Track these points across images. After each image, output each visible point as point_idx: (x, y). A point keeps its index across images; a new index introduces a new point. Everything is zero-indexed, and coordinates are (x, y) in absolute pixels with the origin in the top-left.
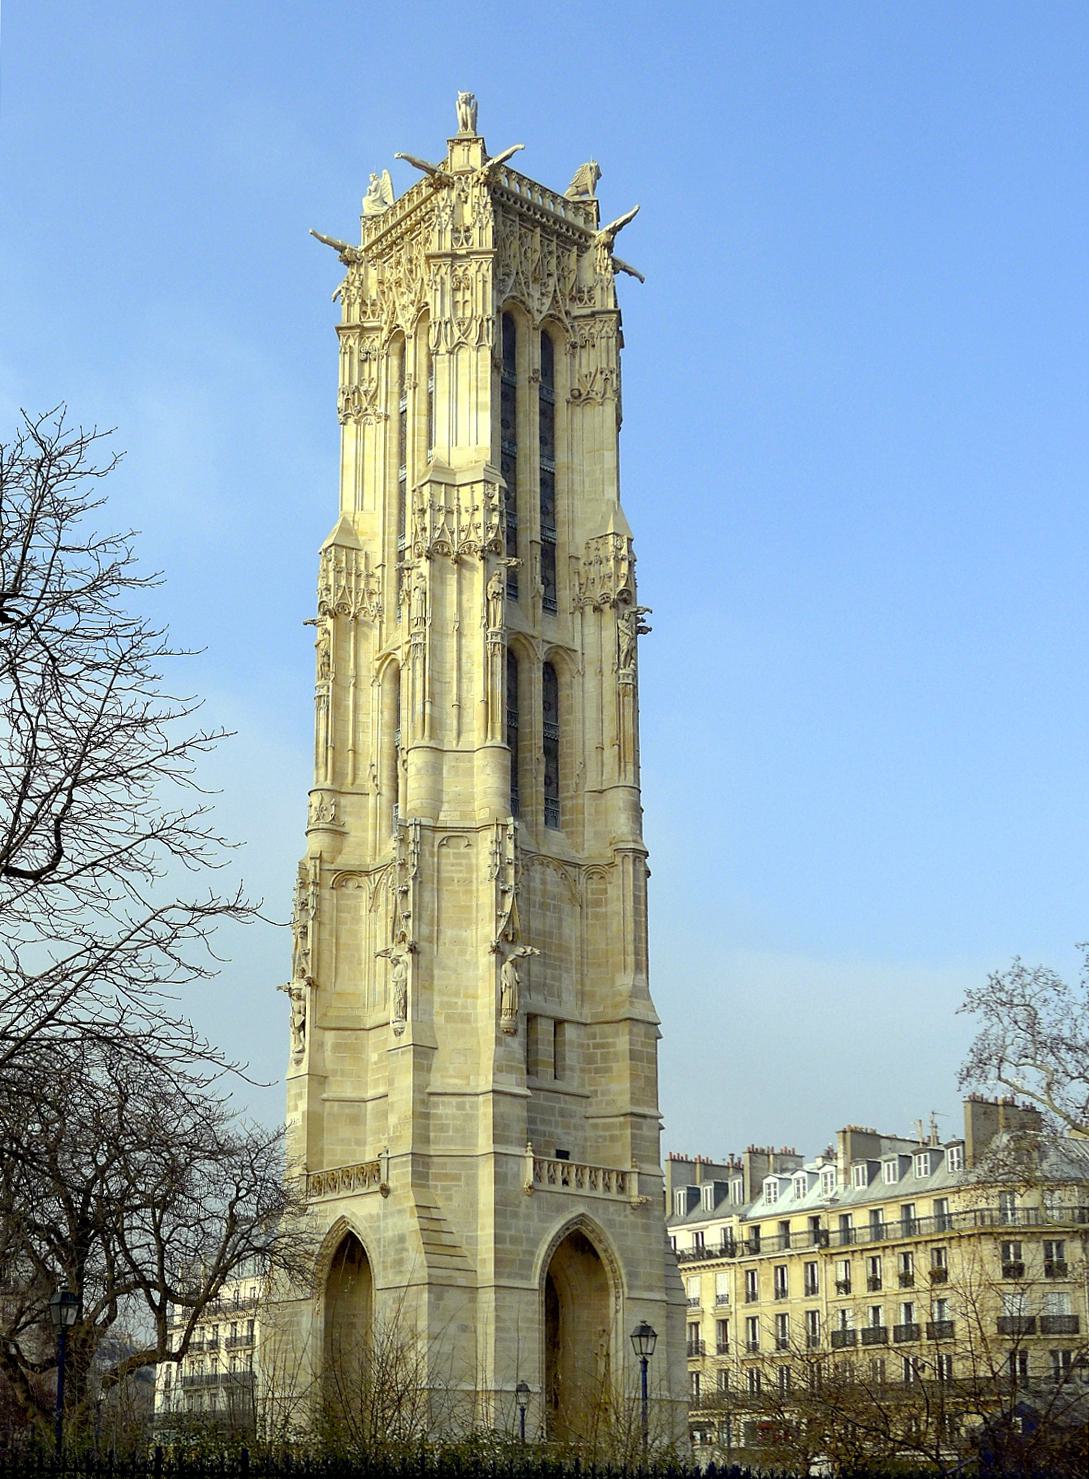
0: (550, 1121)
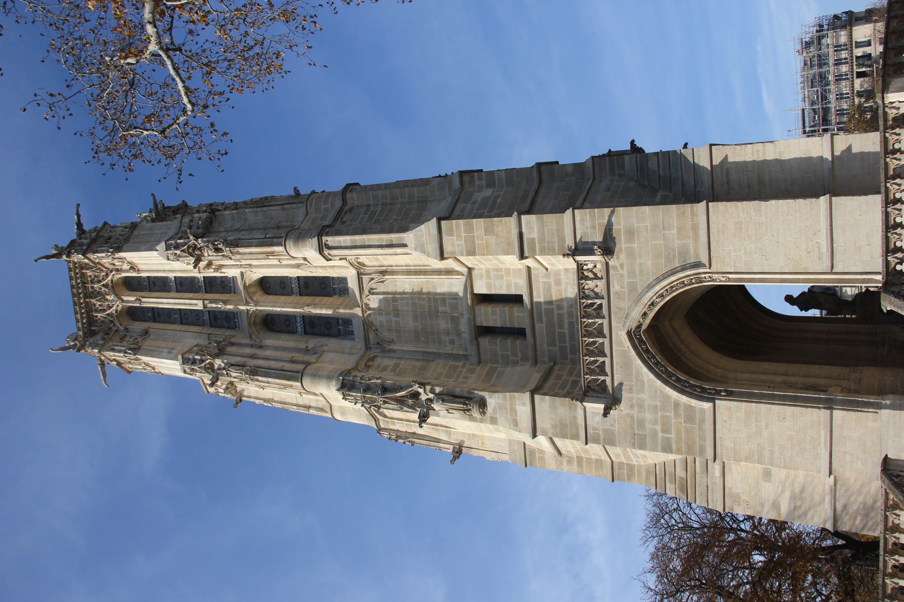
0: (558, 314)
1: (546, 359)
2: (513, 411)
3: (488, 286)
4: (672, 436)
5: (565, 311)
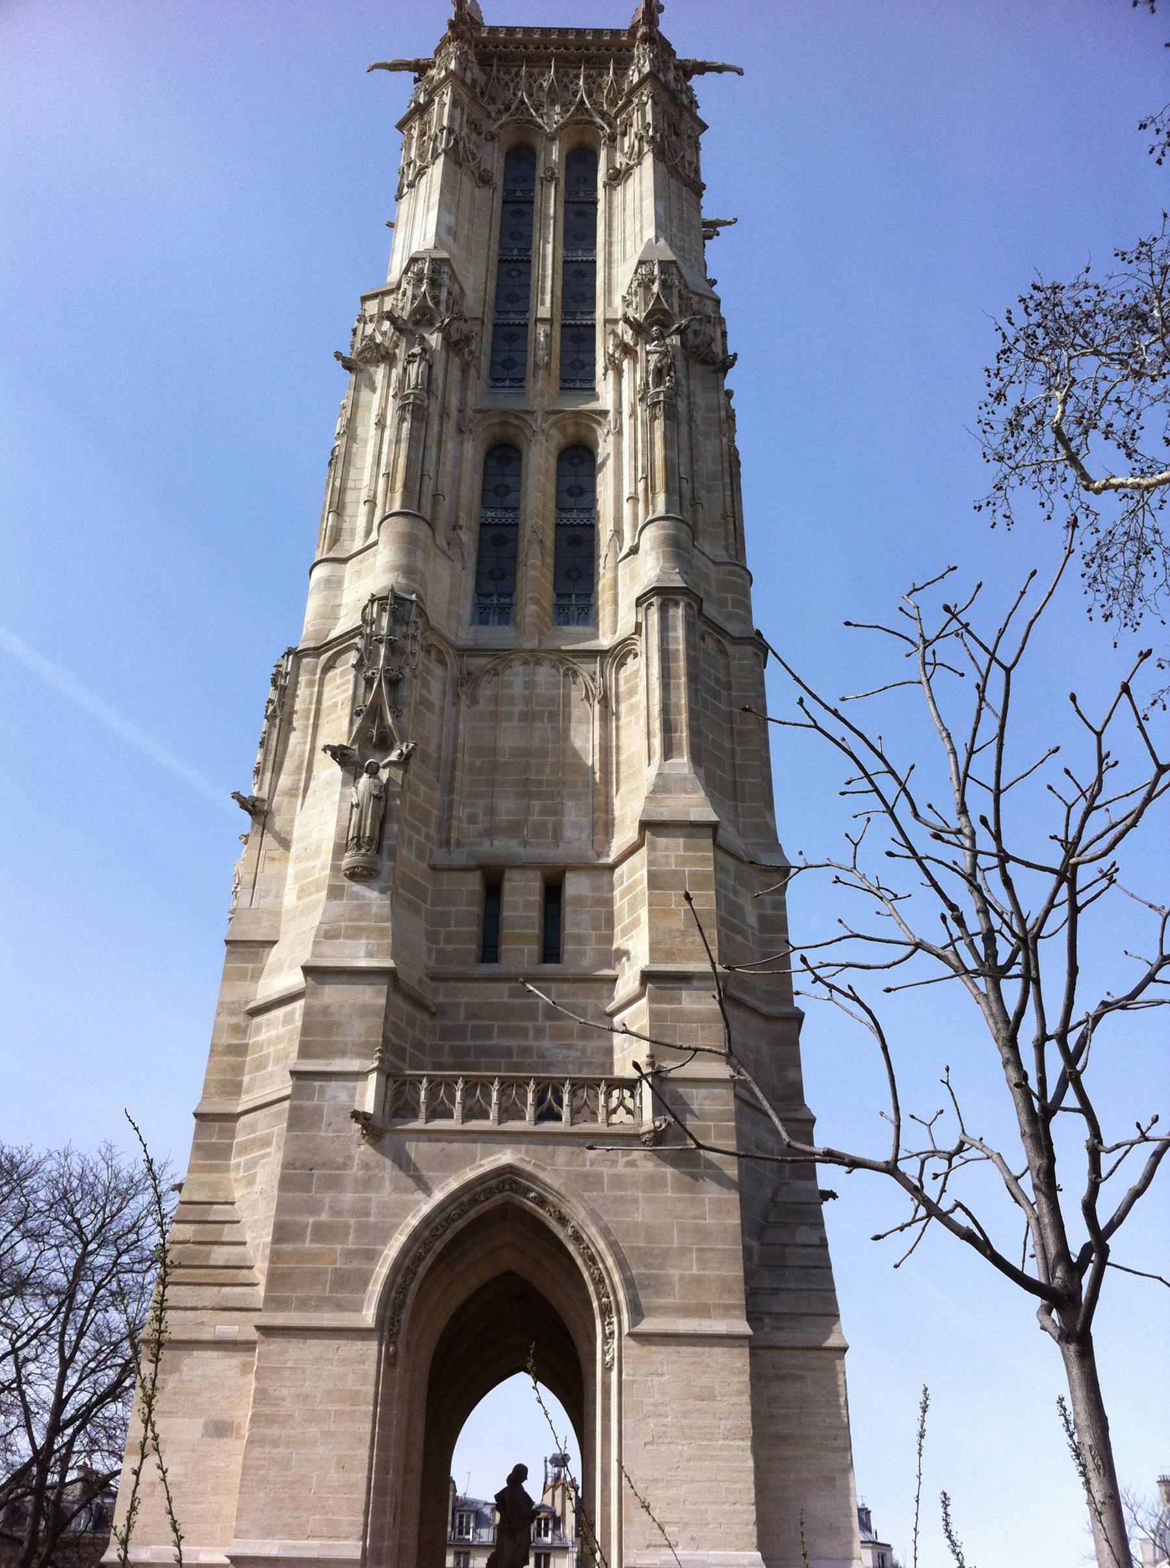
1: (441, 999)
2: (356, 933)
3: (579, 900)
4: (308, 1245)
5: (531, 1042)
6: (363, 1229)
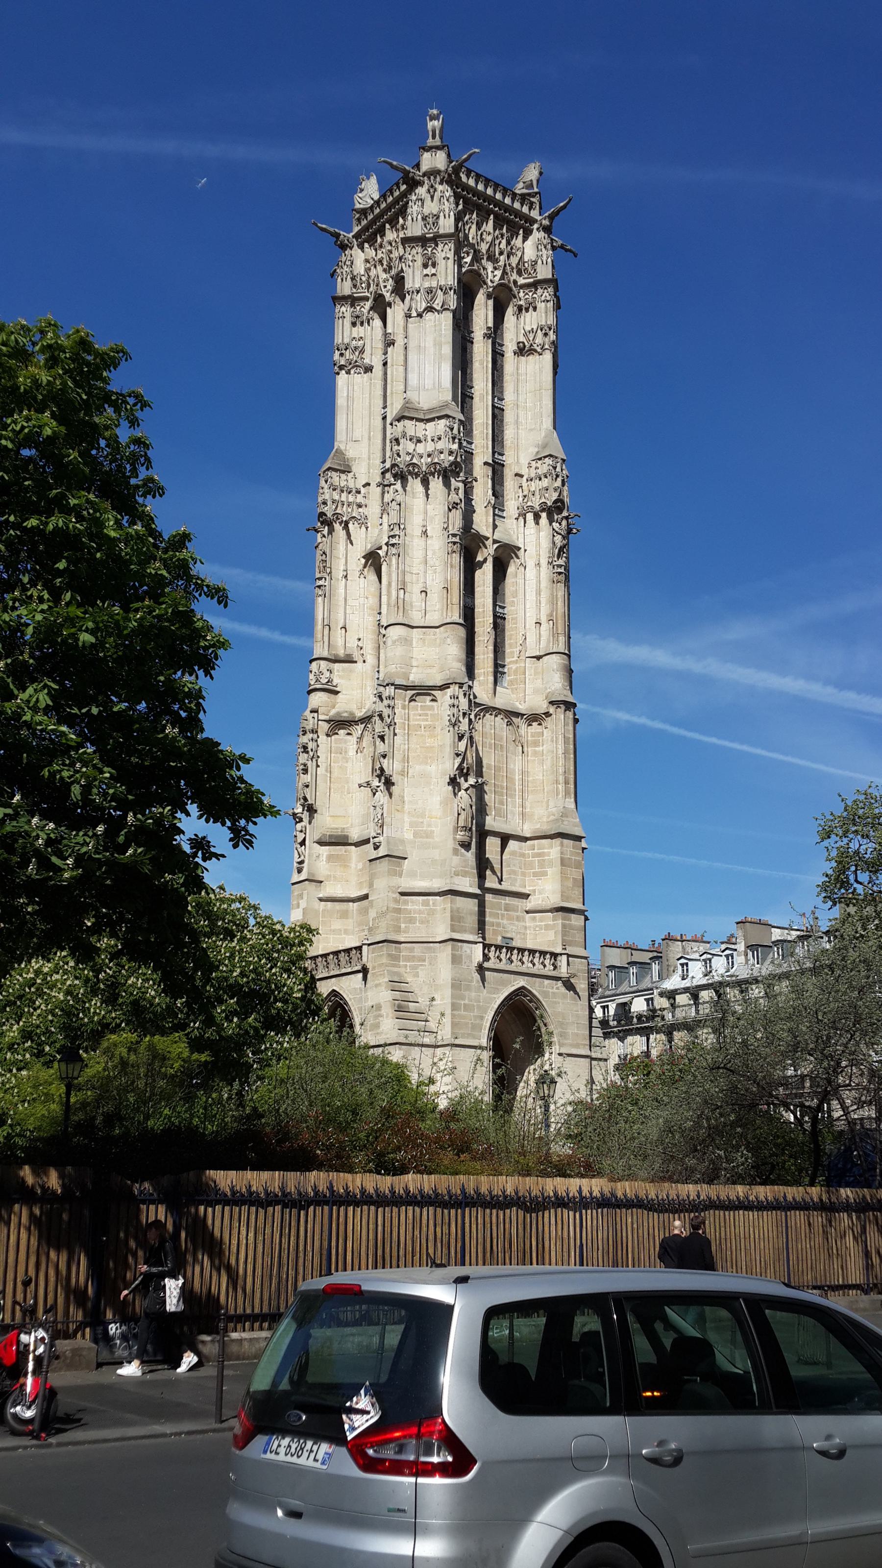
2: (465, 874)
6: (479, 1007)
